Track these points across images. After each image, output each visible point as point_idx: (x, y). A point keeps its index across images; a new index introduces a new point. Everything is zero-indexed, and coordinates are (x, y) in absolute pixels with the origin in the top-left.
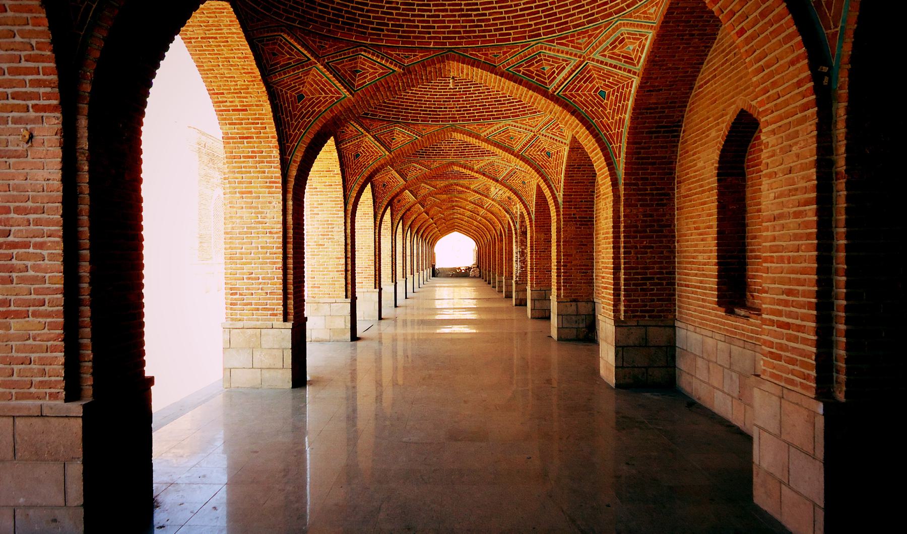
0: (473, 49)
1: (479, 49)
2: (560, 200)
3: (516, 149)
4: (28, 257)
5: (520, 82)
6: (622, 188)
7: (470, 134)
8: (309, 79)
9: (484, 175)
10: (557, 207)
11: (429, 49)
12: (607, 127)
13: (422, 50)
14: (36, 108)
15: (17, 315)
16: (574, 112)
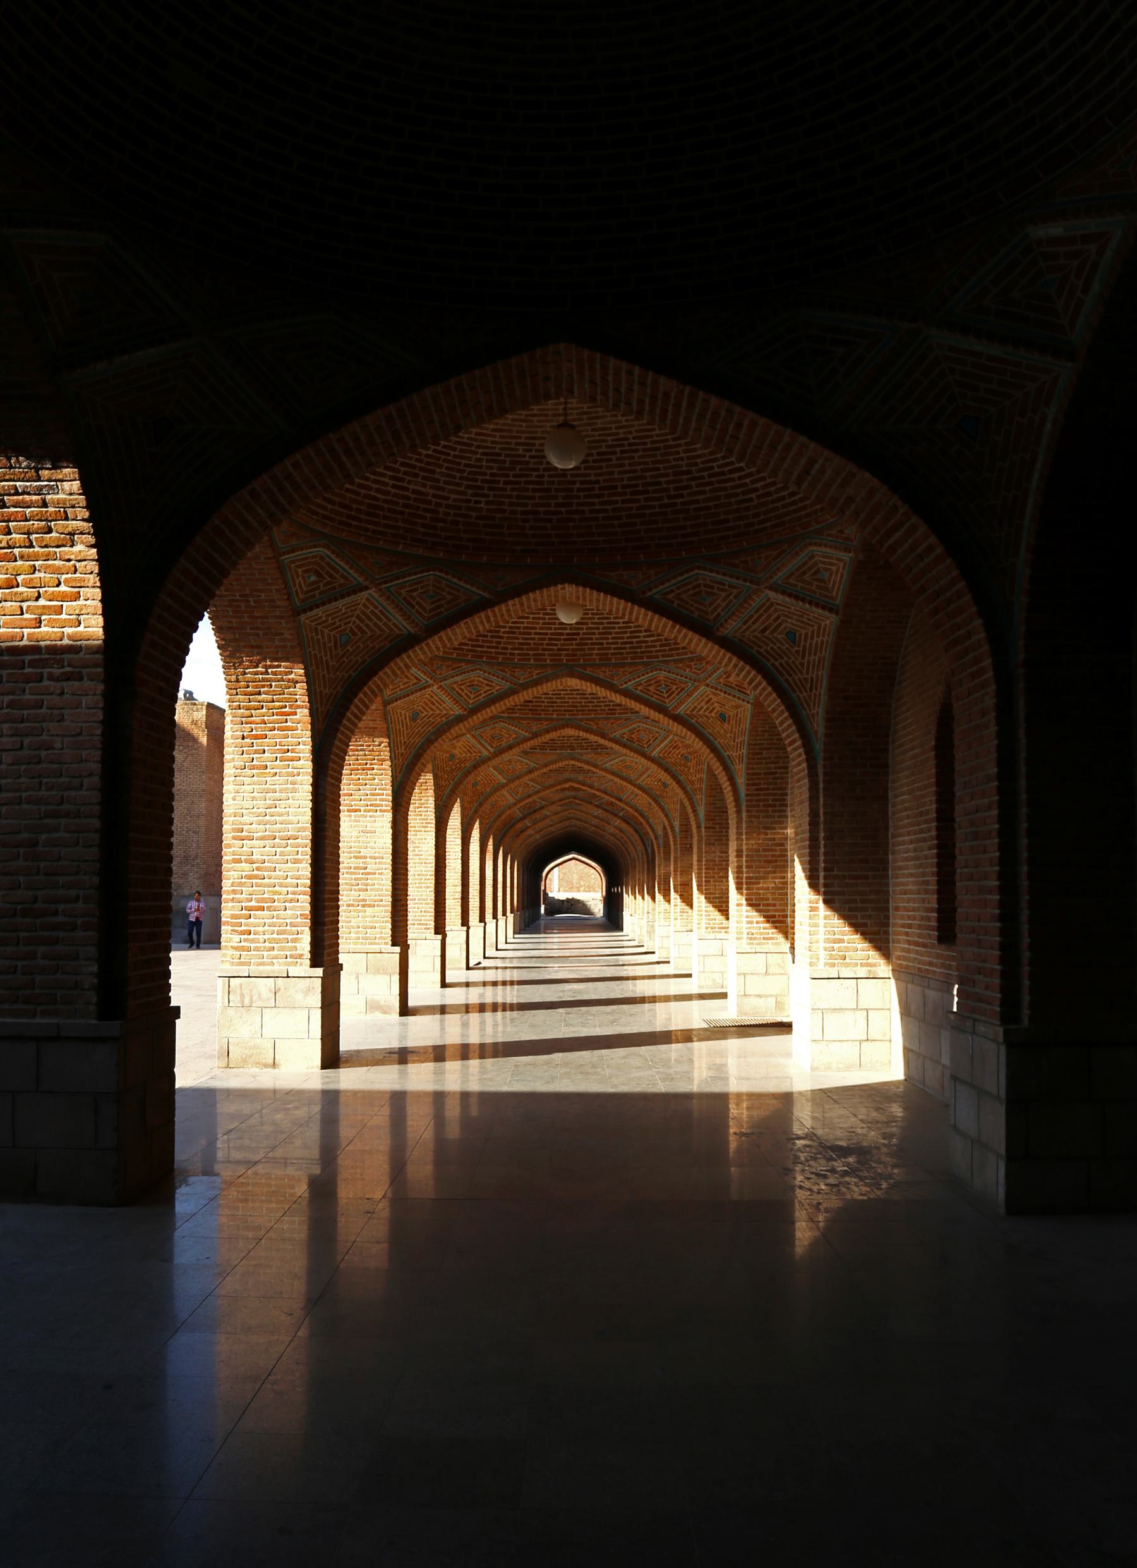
0: (588, 719)
1: (592, 720)
2: (677, 829)
3: (633, 777)
4: (375, 879)
5: (625, 746)
6: (703, 830)
7: (588, 763)
8: (460, 744)
9: (606, 793)
10: (674, 837)
11: (552, 720)
12: (692, 783)
13: (546, 720)
14: (381, 811)
15: (370, 906)
16: (667, 770)
